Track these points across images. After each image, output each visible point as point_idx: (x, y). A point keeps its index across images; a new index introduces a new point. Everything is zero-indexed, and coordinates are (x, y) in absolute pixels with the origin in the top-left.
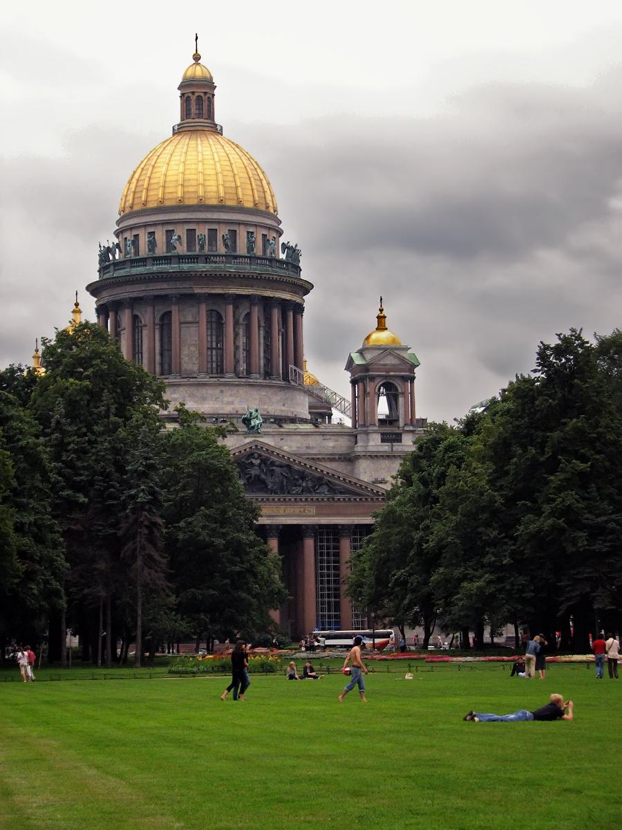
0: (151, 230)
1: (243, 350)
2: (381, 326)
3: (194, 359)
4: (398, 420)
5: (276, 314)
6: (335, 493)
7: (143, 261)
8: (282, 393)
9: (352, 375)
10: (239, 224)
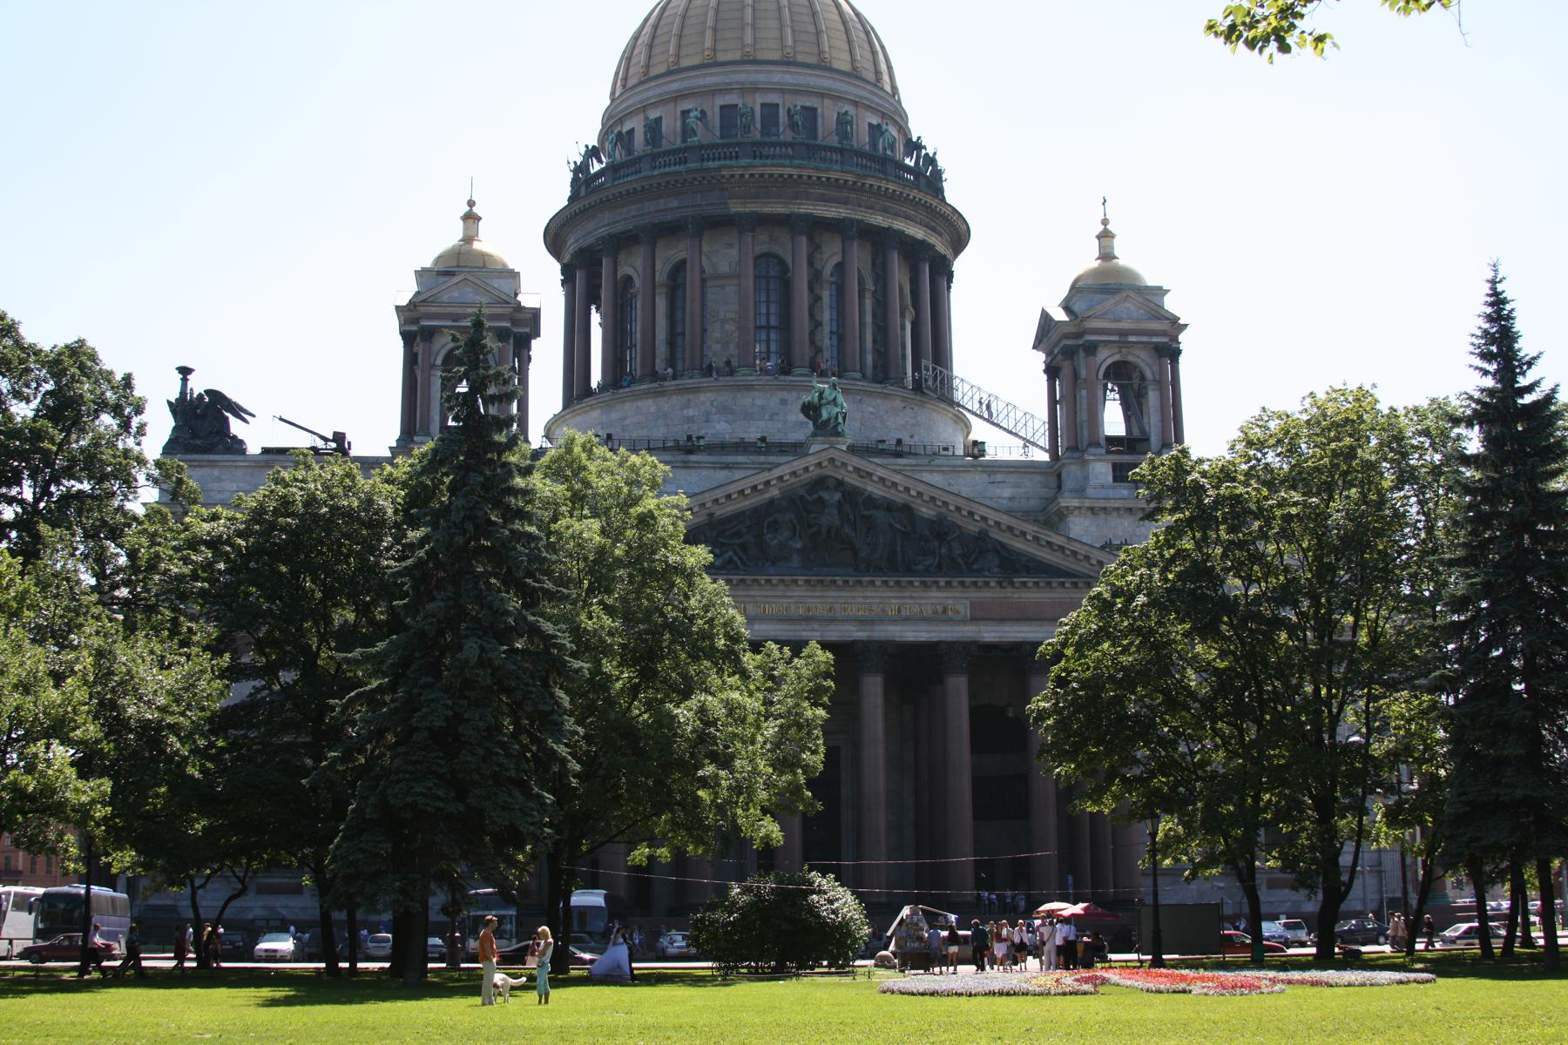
0: (653, 115)
2: (1106, 255)
3: (732, 346)
4: (1148, 440)
6: (1016, 572)
7: (639, 160)
8: (908, 411)
10: (822, 95)
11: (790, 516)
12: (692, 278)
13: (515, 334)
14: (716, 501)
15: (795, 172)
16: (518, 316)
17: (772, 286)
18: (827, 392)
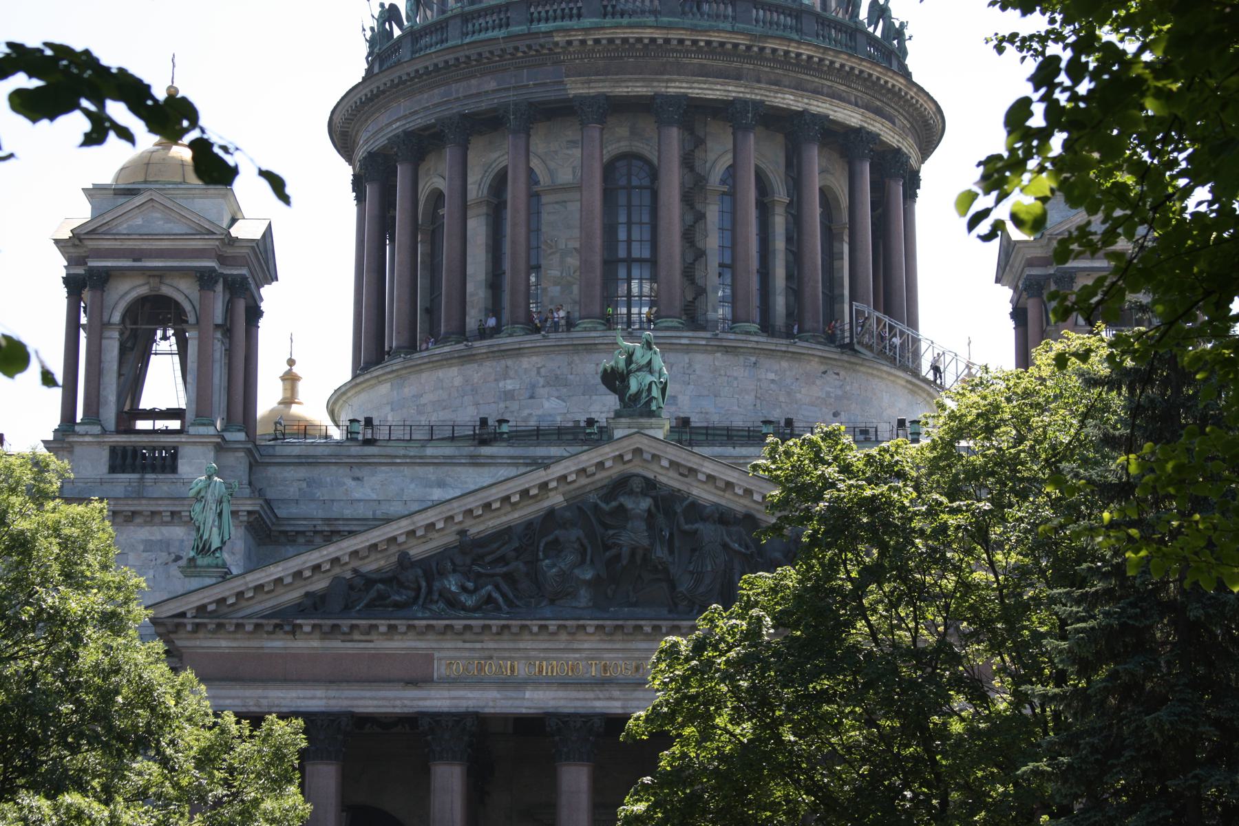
1: (721, 265)
3: (575, 289)
5: (815, 158)
8: (831, 377)
9: (1015, 289)
11: (575, 533)
12: (516, 193)
13: (225, 277)
14: (470, 511)
15: (658, 35)
16: (230, 251)
17: (635, 201)
18: (638, 355)
